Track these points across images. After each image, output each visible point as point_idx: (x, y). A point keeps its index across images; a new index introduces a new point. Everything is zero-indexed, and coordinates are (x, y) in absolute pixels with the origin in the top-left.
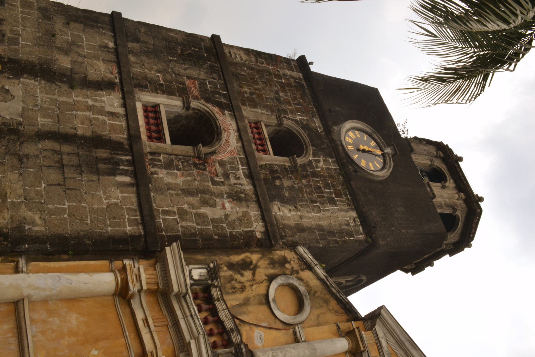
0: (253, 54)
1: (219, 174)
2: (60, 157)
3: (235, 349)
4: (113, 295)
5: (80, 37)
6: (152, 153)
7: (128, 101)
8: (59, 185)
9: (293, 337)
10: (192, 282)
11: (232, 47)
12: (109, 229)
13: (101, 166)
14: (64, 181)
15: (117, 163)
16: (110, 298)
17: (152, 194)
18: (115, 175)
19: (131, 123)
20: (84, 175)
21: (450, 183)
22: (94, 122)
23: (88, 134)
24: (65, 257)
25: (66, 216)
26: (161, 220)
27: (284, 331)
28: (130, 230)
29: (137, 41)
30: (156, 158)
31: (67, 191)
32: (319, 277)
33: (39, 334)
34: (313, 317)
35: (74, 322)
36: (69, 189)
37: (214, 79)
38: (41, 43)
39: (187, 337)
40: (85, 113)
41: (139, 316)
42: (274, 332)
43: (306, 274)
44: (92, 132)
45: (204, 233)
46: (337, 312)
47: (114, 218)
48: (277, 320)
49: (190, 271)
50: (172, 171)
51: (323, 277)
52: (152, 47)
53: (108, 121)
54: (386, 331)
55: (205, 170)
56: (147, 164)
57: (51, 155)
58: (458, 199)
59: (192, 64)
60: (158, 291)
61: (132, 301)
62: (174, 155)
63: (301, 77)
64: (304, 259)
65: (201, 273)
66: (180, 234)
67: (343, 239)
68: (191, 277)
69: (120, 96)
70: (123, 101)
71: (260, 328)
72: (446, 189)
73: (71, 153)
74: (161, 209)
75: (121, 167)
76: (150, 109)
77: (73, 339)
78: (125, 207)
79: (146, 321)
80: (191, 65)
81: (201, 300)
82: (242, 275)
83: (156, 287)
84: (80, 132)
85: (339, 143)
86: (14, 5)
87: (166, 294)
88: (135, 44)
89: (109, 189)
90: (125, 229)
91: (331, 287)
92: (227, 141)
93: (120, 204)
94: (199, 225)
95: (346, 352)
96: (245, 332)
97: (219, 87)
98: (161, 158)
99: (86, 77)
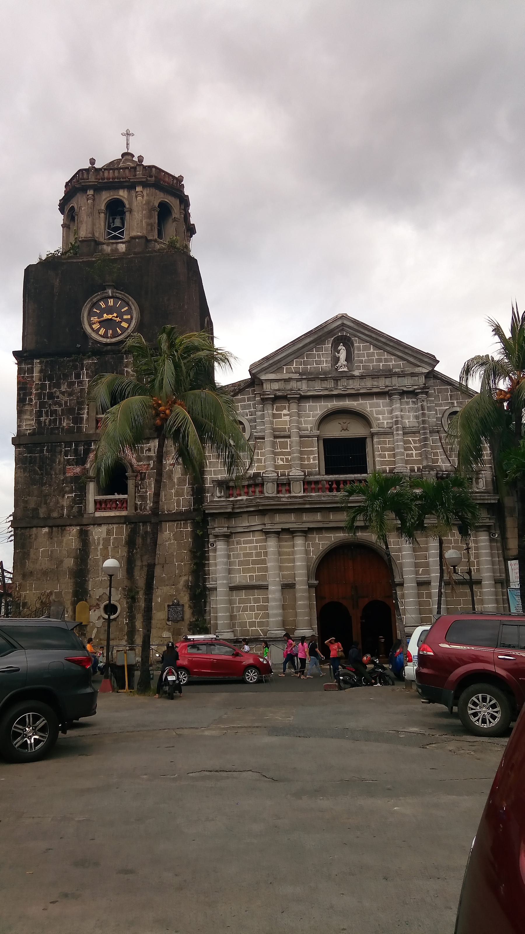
0: (23, 407)
2: (144, 566)
6: (136, 509)
8: (163, 567)
11: (19, 426)
12: (190, 540)
14: (161, 564)
21: (123, 194)
22: (116, 545)
25: (182, 564)
30: (139, 506)
31: (167, 562)
36: (165, 561)
37: (61, 451)
40: (110, 550)
45: (191, 482)
50: (148, 496)
55: (145, 473)
58: (143, 197)
62: (135, 494)
63: (38, 361)
69: (92, 526)
72: (132, 208)
73: (141, 559)
76: (98, 506)
78: (176, 530)
86: (25, 596)
89: (164, 538)
93: (174, 533)
97: (69, 449)
98: (139, 503)
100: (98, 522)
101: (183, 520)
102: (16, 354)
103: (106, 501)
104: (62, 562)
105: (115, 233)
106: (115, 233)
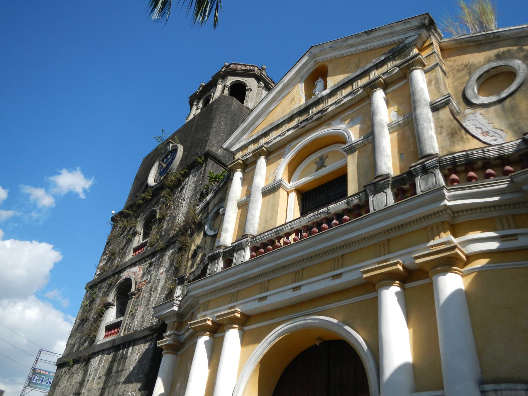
1: (147, 278)
4: (177, 355)
7: (97, 350)
13: (120, 369)
16: (178, 358)
17: (143, 328)
19: (106, 347)
22: (100, 376)
23: (104, 378)
28: (153, 344)
29: (74, 344)
32: (214, 196)
43: (211, 207)
51: (213, 193)
52: (79, 334)
53: (102, 364)
54: (238, 143)
56: (128, 333)
60: (180, 321)
61: (181, 341)
64: (202, 209)
65: (181, 289)
67: (201, 179)
70: (97, 354)
75: (124, 353)
83: (176, 323)
84: (101, 385)
85: (155, 187)
87: (182, 315)
90: (152, 348)
91: (220, 187)
92: (134, 273)
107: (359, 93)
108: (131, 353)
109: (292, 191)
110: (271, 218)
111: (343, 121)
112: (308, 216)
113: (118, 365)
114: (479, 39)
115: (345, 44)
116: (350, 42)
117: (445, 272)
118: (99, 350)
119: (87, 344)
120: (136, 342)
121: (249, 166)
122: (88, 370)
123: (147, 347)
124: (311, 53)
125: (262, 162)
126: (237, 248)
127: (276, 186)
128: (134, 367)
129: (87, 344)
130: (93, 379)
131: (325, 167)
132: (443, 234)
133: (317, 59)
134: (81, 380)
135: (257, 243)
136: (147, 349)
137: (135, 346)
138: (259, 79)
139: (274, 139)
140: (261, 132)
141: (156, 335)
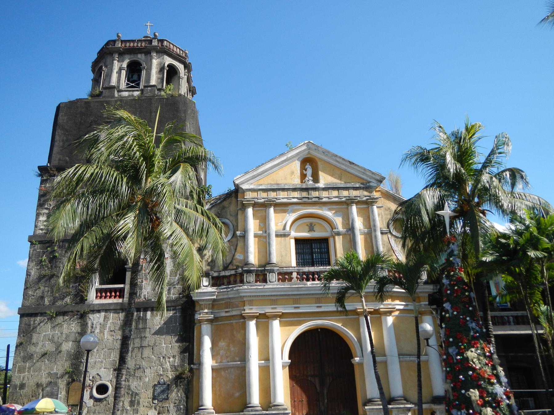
2: (135, 349)
3: (245, 272)
5: (45, 336)
7: (96, 308)
9: (242, 238)
10: (209, 286)
12: (178, 324)
13: (141, 326)
14: (151, 346)
15: (139, 318)
18: (146, 320)
19: (112, 308)
20: (147, 335)
21: (141, 57)
22: (112, 329)
23: (120, 333)
24: (191, 346)
26: (174, 296)
27: (238, 241)
28: (179, 314)
29: (42, 298)
33: (228, 359)
34: (231, 219)
35: (223, 344)
38: (54, 359)
39: (237, 296)
41: (223, 314)
42: (238, 248)
44: (119, 330)
46: (230, 202)
47: (172, 321)
48: (231, 240)
49: (204, 286)
51: (211, 206)
52: (46, 288)
53: (111, 321)
57: (135, 353)
59: (59, 261)
66: (182, 287)
68: (206, 286)
70: (95, 311)
71: (236, 254)
74: (167, 296)
75: (141, 315)
76: (99, 294)
77: (231, 345)
79: (226, 312)
80: (60, 262)
81: (218, 281)
82: (205, 255)
83: (211, 305)
88: (46, 299)
91: (217, 203)
94: (177, 275)
95: (253, 209)
96: (236, 263)
99: (78, 333)
100: (97, 310)
101: (173, 306)
102: (40, 168)
103: (106, 290)
104: (61, 344)
105: (132, 84)
106: (133, 84)
107: (342, 200)
108: (151, 317)
109: (292, 238)
110: (286, 255)
111: (330, 210)
112: (320, 268)
113: (137, 324)
114: (397, 197)
115: (333, 157)
116: (338, 159)
117: (389, 316)
118: (100, 309)
119: (68, 300)
120: (155, 309)
121: (256, 206)
122: (87, 324)
123: (171, 314)
124: (308, 146)
125: (272, 210)
126: (269, 271)
127: (287, 234)
128: (160, 328)
129: (68, 300)
130: (102, 332)
131: (314, 231)
132: (389, 300)
133: (310, 151)
134: (79, 331)
135: (283, 271)
136: (172, 316)
137: (155, 312)
138: (187, 67)
139: (283, 198)
140: (270, 186)
141: (180, 307)
